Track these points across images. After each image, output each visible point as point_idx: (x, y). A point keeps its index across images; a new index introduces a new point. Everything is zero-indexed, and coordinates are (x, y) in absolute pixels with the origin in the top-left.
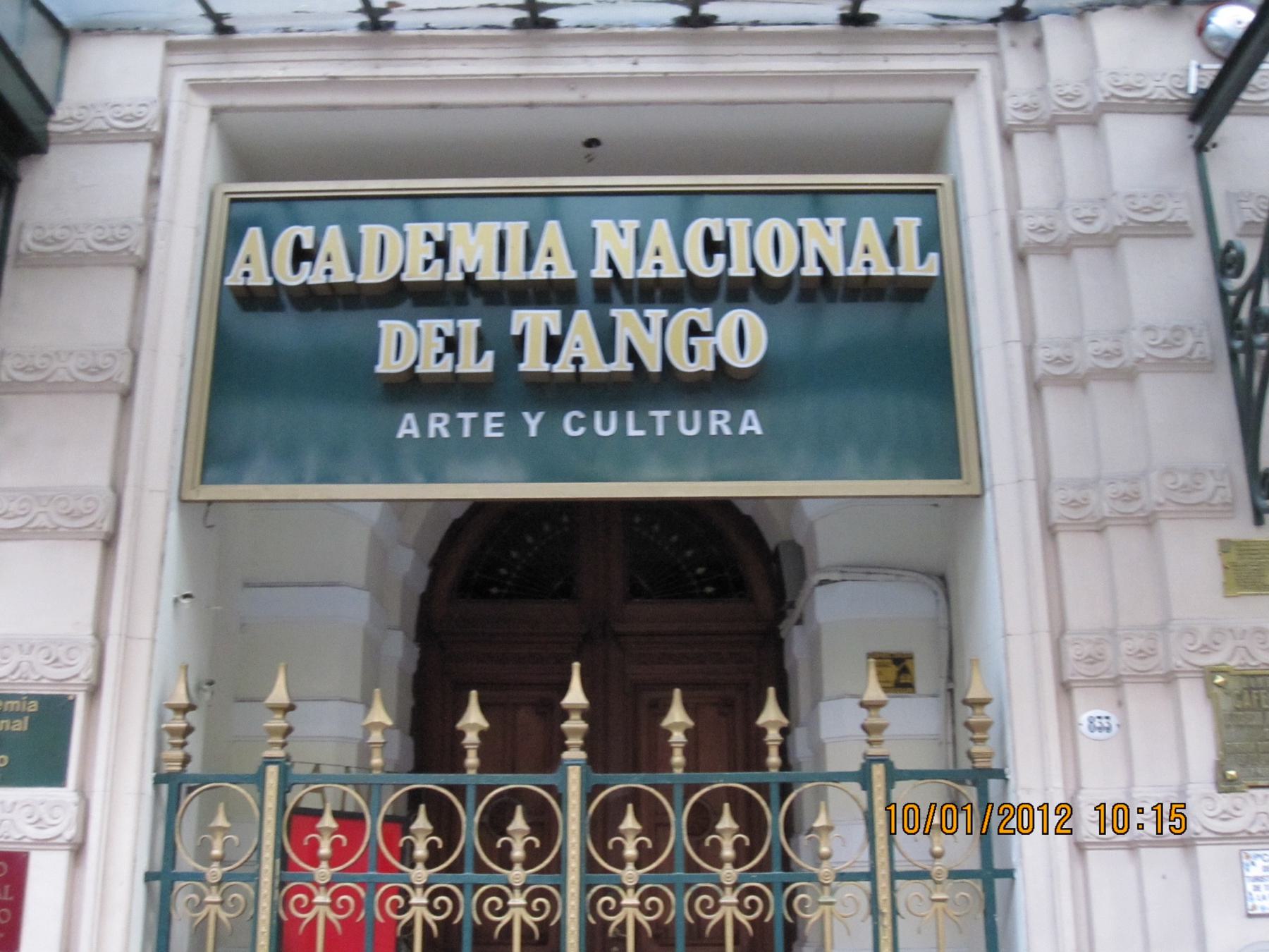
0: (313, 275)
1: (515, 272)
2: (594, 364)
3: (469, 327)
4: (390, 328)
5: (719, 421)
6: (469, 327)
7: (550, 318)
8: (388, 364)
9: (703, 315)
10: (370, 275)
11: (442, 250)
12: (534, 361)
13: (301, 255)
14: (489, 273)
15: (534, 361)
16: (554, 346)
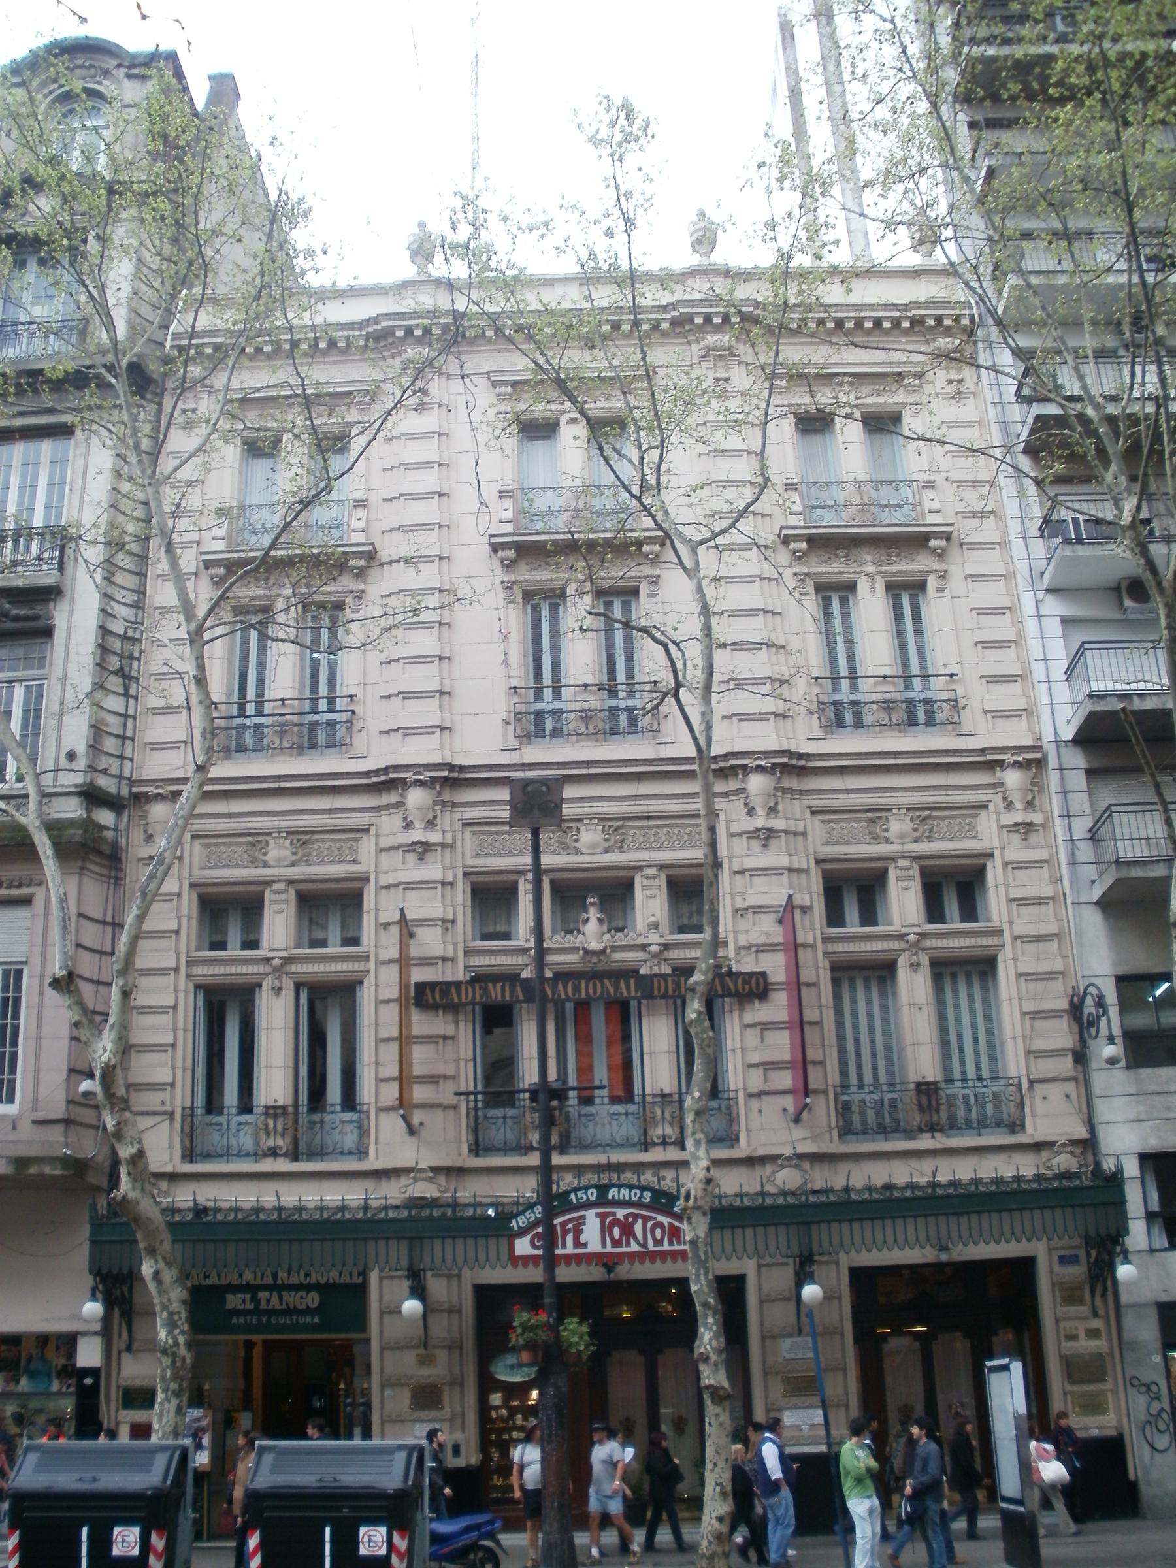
0: (209, 1282)
1: (258, 1282)
2: (278, 1306)
3: (248, 1296)
4: (229, 1297)
5: (309, 1319)
6: (248, 1296)
7: (267, 1294)
8: (229, 1306)
9: (303, 1293)
10: (224, 1282)
11: (241, 1276)
12: (263, 1305)
13: (206, 1277)
14: (252, 1282)
15: (263, 1305)
16: (268, 1302)
